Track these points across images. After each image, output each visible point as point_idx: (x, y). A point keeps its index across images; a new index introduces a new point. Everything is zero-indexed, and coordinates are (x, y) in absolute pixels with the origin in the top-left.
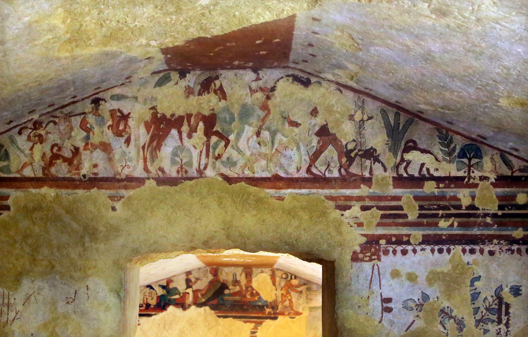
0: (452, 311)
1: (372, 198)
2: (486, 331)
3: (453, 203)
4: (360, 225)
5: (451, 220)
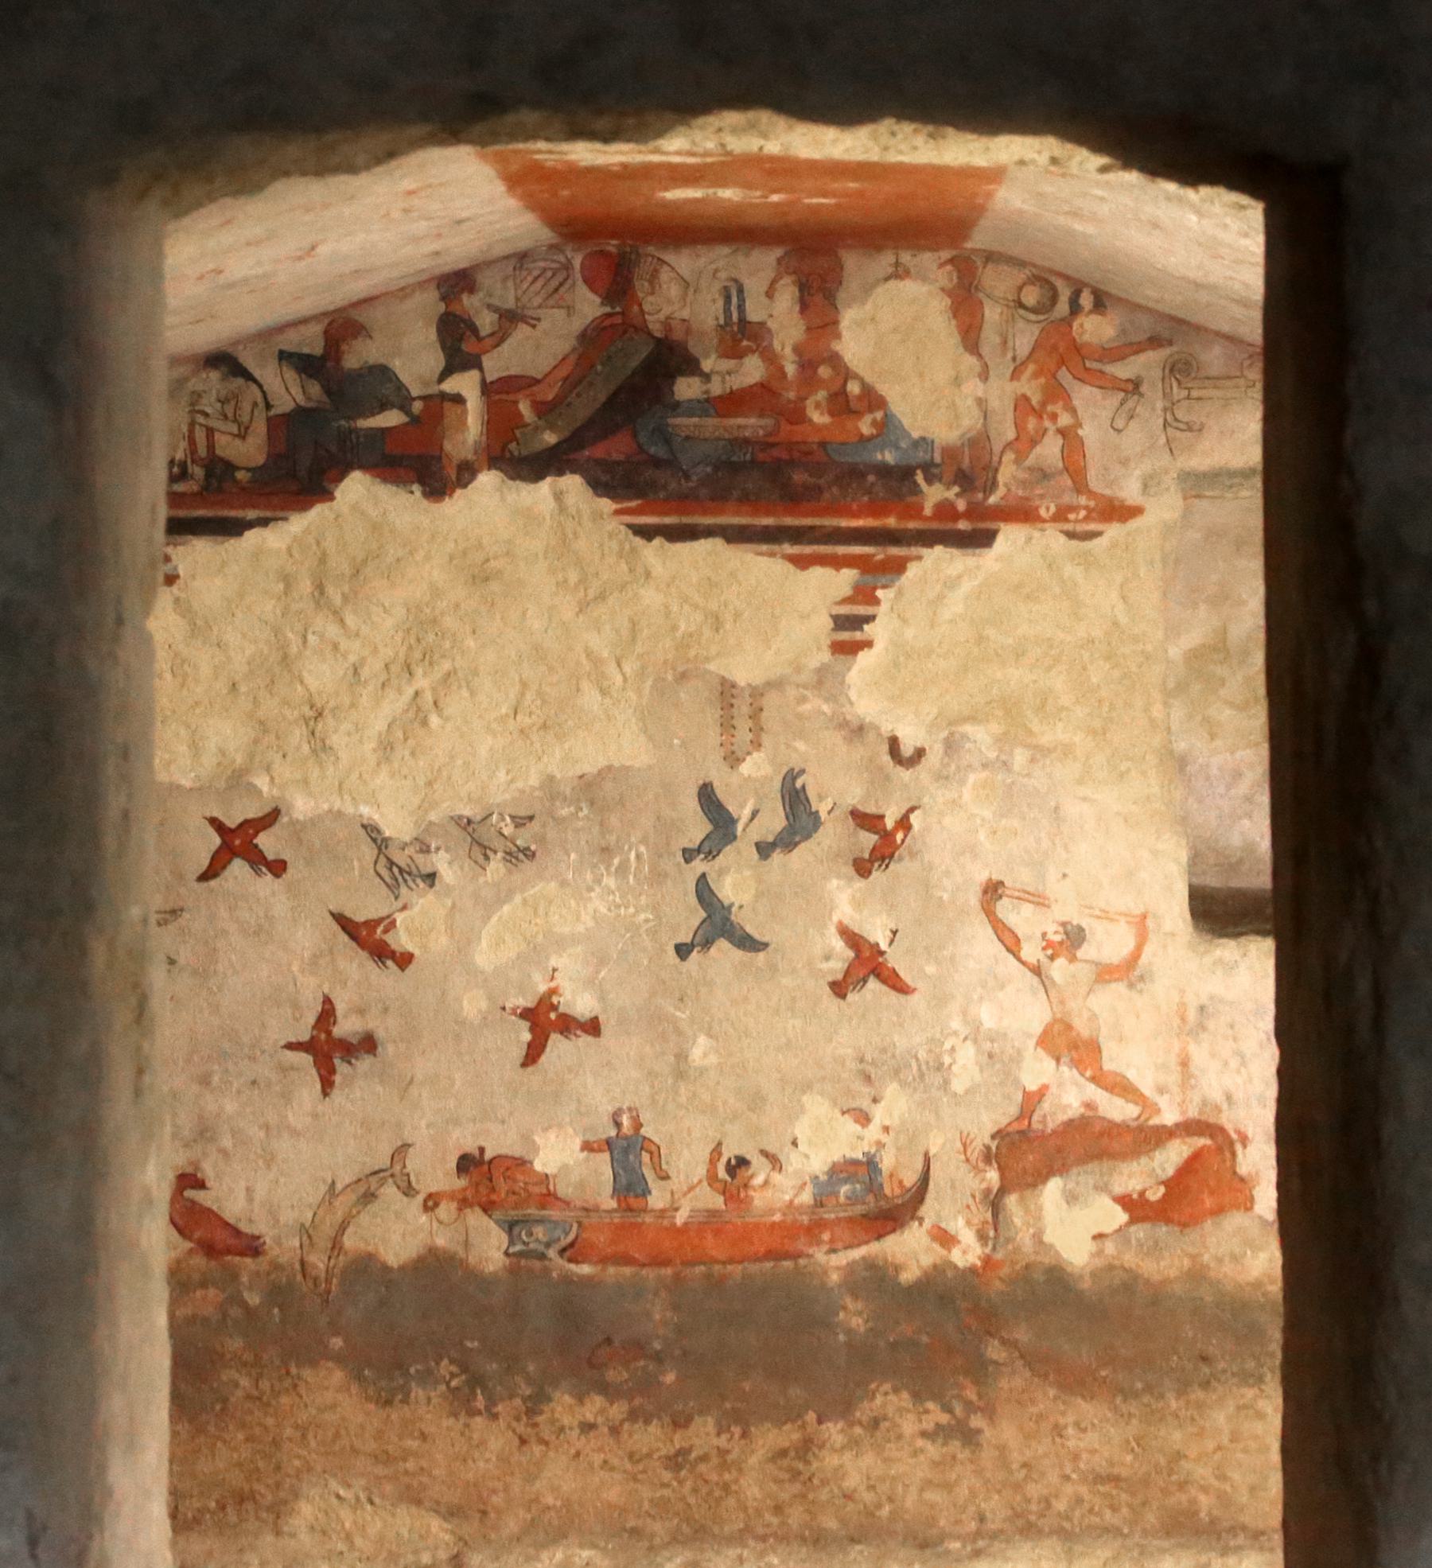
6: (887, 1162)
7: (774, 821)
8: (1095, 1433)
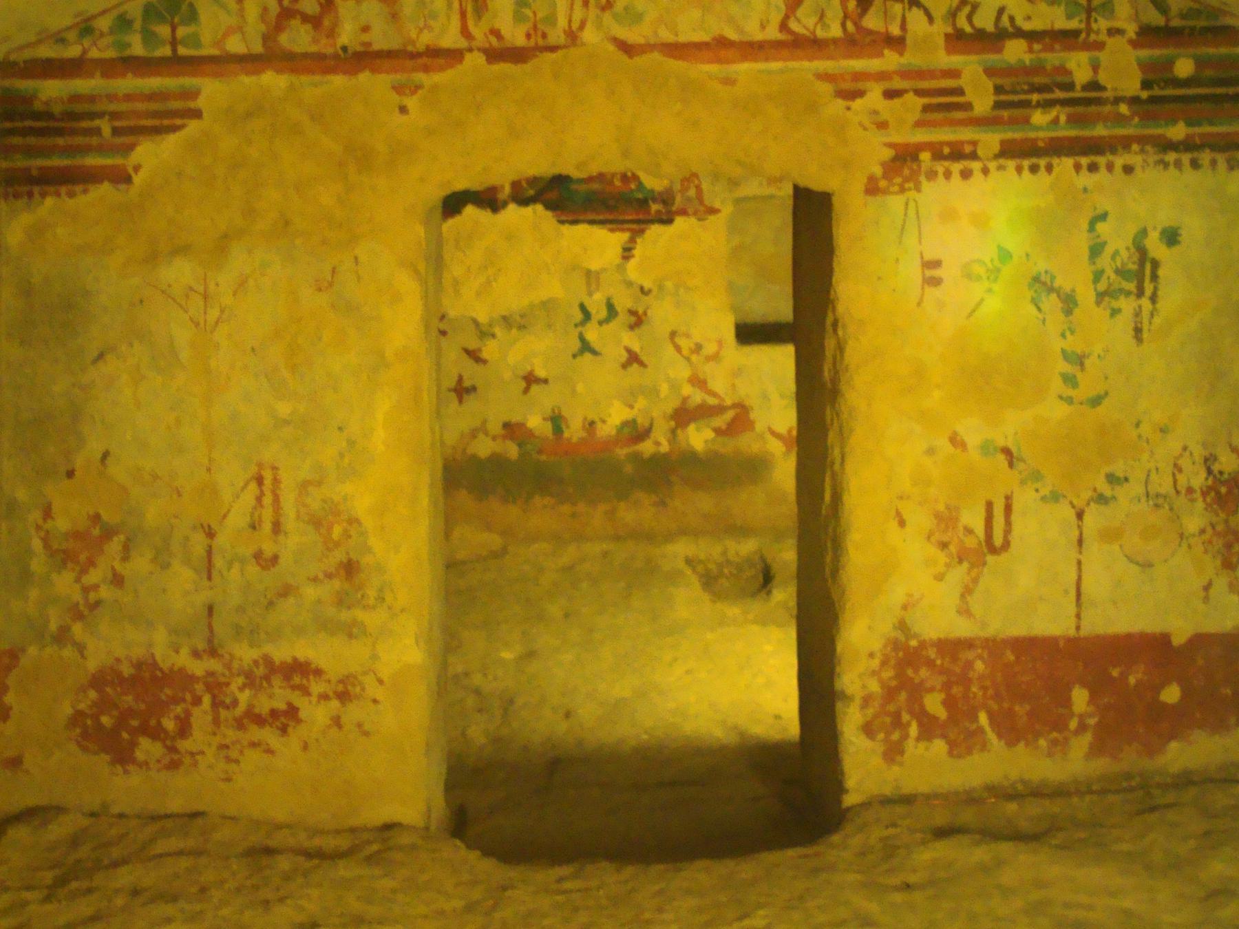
0: (1053, 278)
1: (905, 74)
2: (1115, 312)
3: (1059, 79)
4: (882, 125)
5: (1054, 112)
6: (640, 421)
7: (603, 313)
8: (705, 502)
